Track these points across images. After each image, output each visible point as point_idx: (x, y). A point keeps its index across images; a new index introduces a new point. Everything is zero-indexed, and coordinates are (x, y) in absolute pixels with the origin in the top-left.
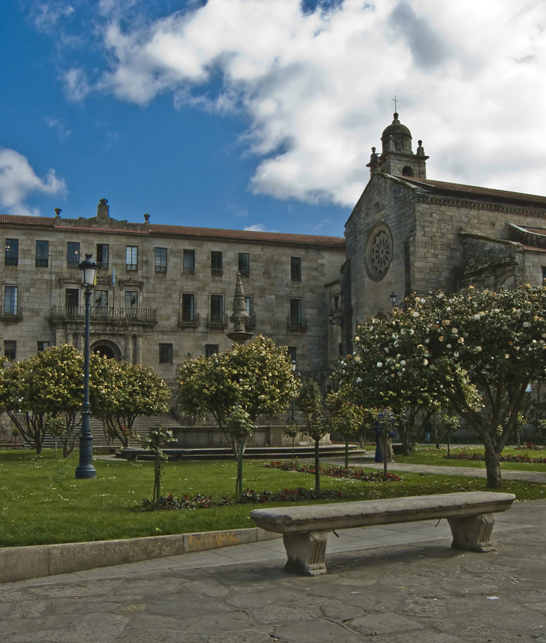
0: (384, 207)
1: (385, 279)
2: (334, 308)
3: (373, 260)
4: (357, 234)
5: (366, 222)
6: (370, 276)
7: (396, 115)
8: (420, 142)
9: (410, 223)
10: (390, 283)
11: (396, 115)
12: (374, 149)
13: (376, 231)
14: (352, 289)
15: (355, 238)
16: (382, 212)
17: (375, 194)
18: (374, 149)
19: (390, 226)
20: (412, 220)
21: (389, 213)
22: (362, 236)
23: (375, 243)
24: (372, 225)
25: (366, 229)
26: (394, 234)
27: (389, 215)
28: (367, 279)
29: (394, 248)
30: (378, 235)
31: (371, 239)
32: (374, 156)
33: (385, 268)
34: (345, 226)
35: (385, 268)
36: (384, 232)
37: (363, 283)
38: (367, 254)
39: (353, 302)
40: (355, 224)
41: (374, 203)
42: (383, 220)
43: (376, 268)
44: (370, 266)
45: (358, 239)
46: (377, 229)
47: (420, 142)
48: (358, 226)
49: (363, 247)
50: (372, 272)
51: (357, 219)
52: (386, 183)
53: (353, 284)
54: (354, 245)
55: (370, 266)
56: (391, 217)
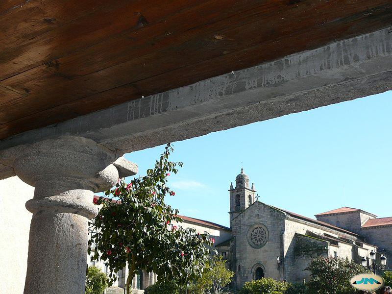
0: (262, 217)
1: (263, 249)
3: (252, 239)
7: (242, 169)
8: (253, 184)
10: (267, 251)
11: (242, 169)
12: (232, 183)
13: (256, 226)
18: (232, 183)
20: (282, 226)
22: (245, 227)
23: (254, 231)
29: (270, 237)
30: (257, 228)
31: (252, 229)
32: (232, 186)
33: (261, 244)
35: (261, 244)
36: (260, 228)
37: (246, 248)
39: (238, 256)
40: (240, 221)
42: (262, 222)
43: (254, 243)
47: (253, 184)
50: (252, 243)
51: (241, 219)
53: (237, 248)
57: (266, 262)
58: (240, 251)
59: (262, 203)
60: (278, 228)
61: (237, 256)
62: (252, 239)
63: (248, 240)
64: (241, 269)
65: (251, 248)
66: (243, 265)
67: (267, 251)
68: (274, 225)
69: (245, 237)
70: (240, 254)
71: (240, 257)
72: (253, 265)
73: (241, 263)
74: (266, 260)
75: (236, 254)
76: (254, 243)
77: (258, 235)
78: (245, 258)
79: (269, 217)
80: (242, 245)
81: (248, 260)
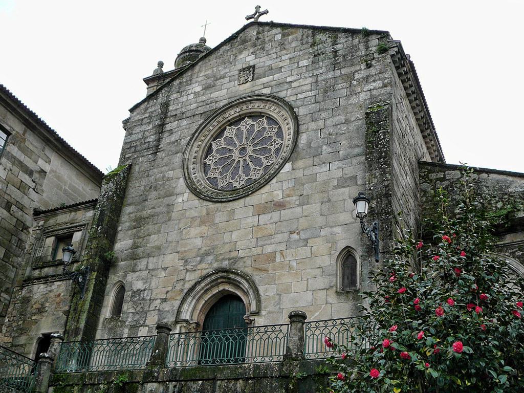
2: (50, 258)
4: (168, 120)
5: (204, 98)
6: (196, 192)
9: (370, 90)
10: (280, 206)
13: (232, 114)
14: (124, 218)
15: (162, 125)
16: (265, 80)
17: (245, 53)
19: (291, 99)
21: (289, 79)
22: (185, 122)
24: (222, 104)
25: (201, 110)
26: (301, 112)
27: (291, 82)
28: (184, 199)
29: (303, 139)
31: (213, 128)
34: (131, 110)
38: (195, 154)
39: (122, 244)
40: (166, 105)
41: (240, 67)
42: (267, 91)
44: (197, 175)
45: (168, 127)
46: (238, 110)
48: (171, 108)
49: (184, 142)
52: (283, 35)
53: (128, 210)
54: (152, 138)
55: (197, 175)
56: (294, 85)
57: (271, 257)
58: (139, 222)
59: (272, 25)
60: (348, 97)
61: (118, 246)
62: (206, 168)
63: (184, 165)
64: (125, 307)
65: (196, 202)
66: (139, 285)
67: (280, 206)
68: (328, 90)
69: (178, 158)
70: (135, 236)
71: (135, 247)
72: (192, 278)
73: (130, 277)
74: (269, 249)
75: (120, 236)
76: (213, 181)
77: (236, 154)
78: (159, 250)
79: (304, 63)
80: (154, 194)
81: (171, 259)
